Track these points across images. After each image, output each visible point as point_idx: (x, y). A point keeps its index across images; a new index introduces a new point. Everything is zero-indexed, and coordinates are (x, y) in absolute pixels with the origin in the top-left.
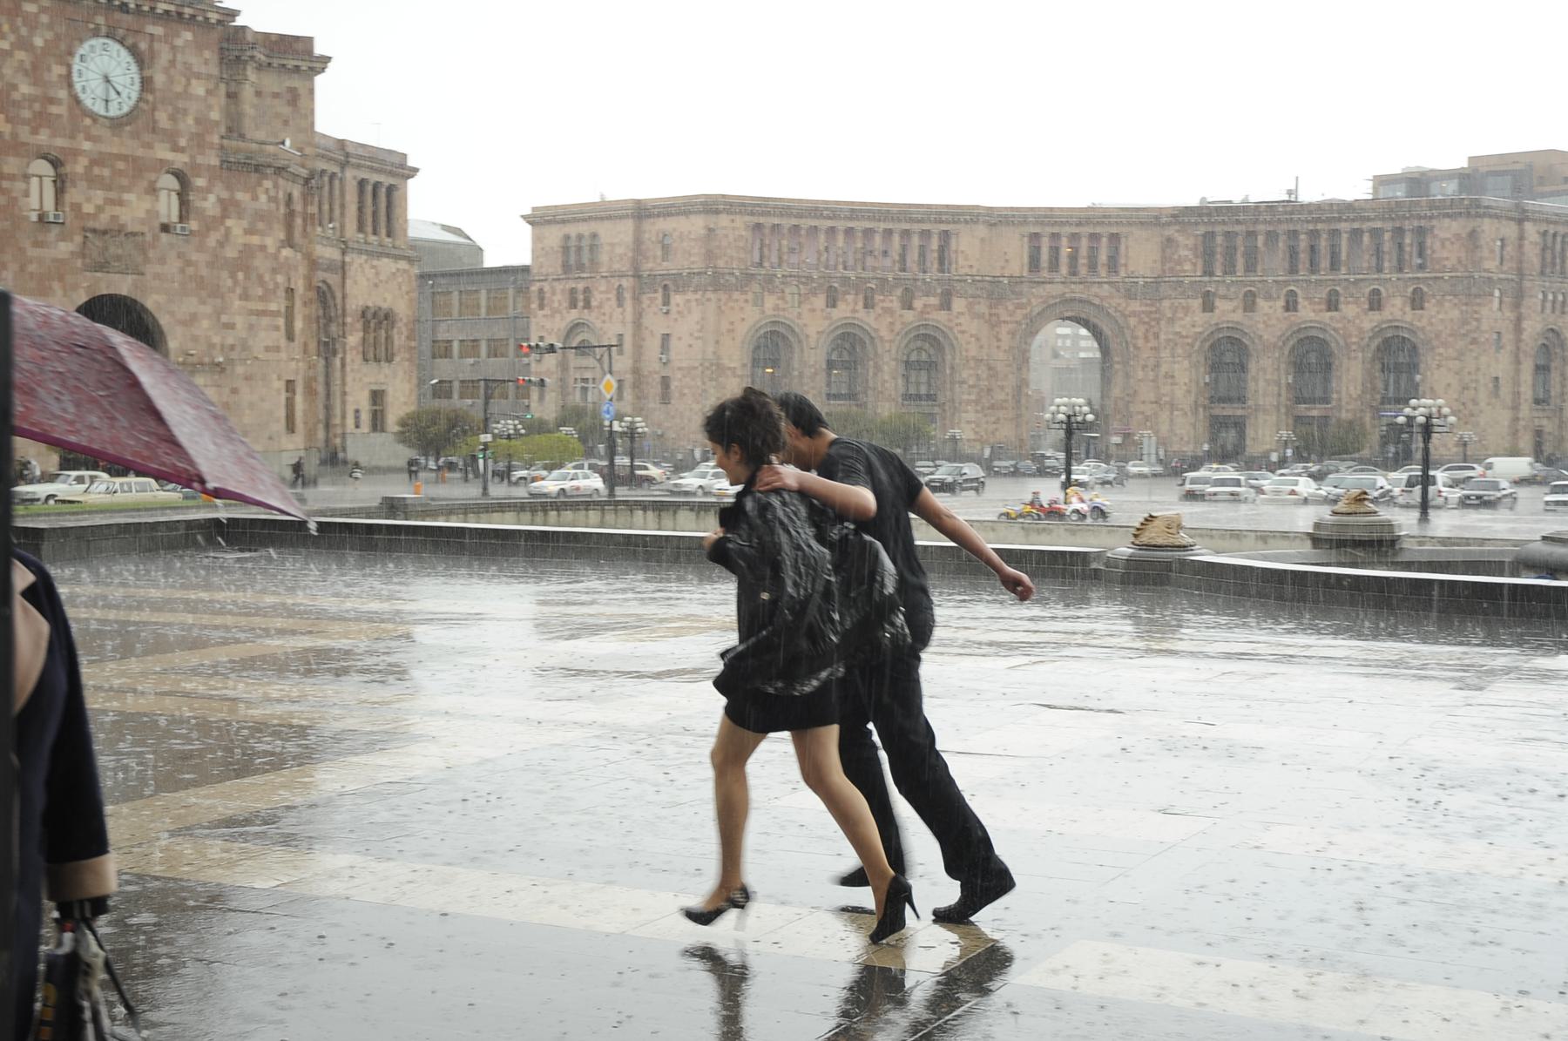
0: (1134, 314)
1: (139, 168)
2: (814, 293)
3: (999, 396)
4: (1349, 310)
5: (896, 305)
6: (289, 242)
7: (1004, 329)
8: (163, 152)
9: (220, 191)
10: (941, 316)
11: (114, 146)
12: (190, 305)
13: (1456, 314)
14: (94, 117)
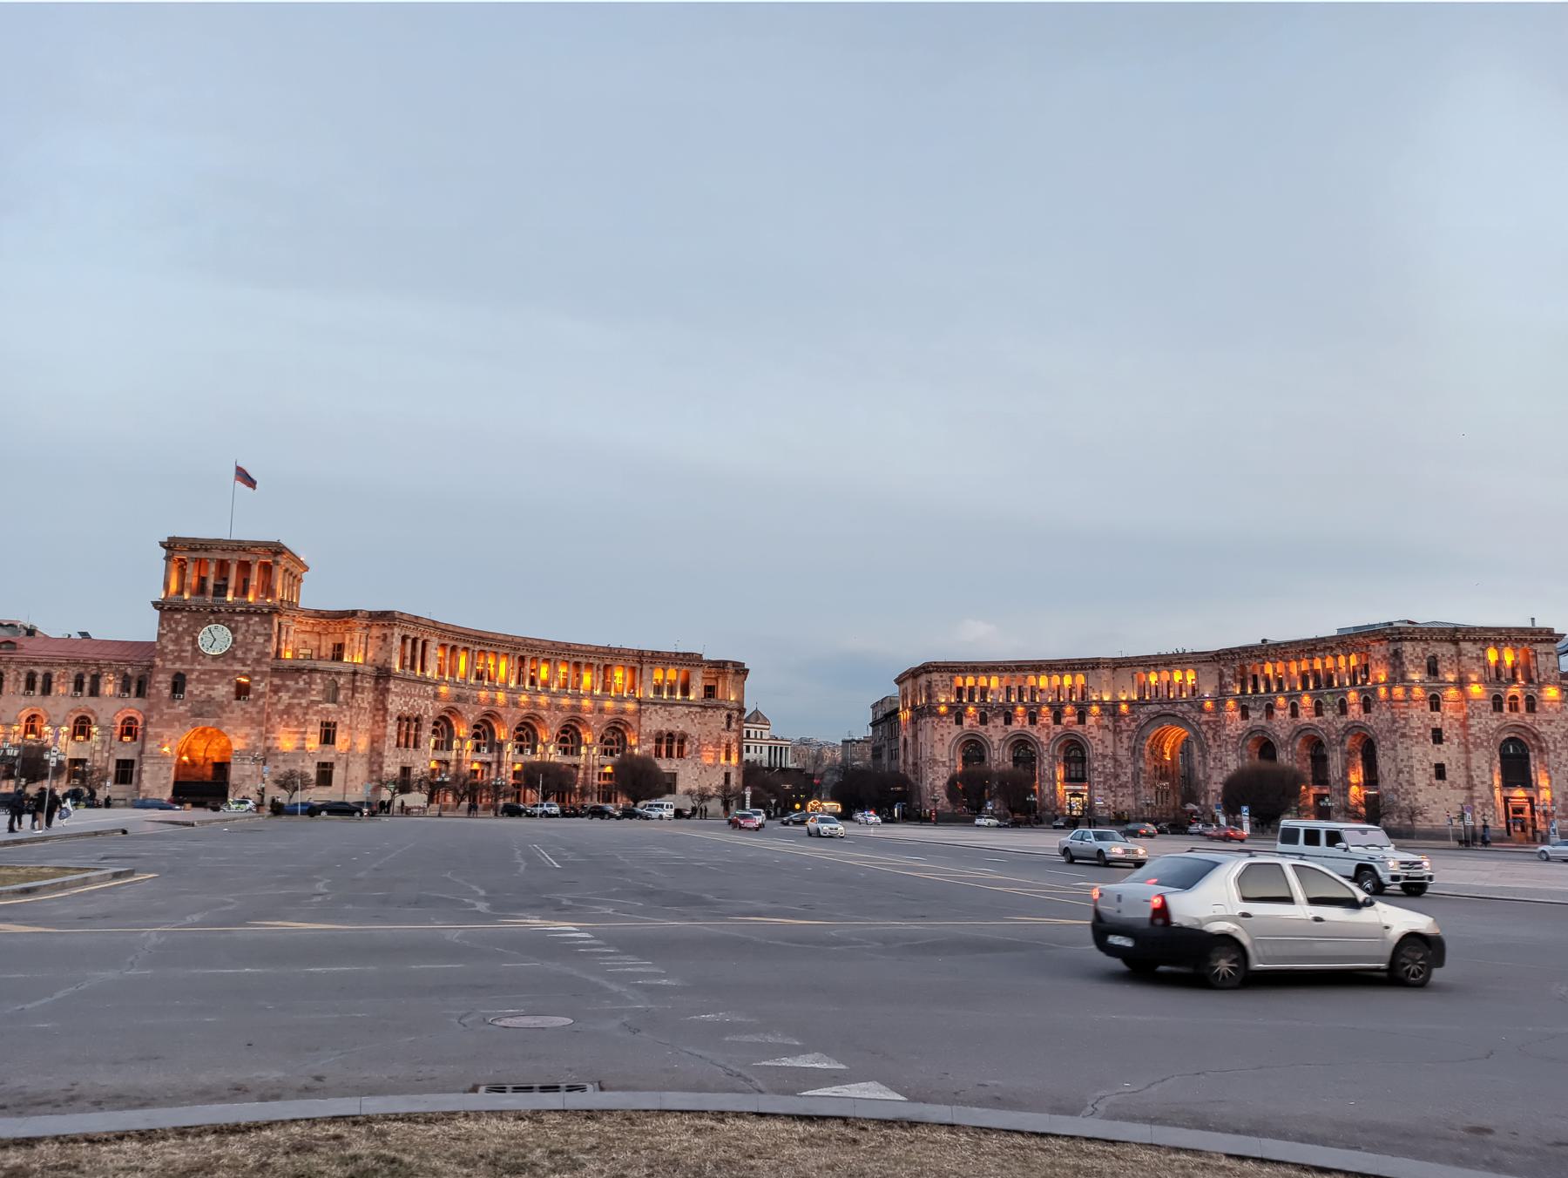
0: (1207, 723)
1: (223, 674)
2: (996, 716)
3: (1124, 779)
4: (1329, 715)
5: (1051, 722)
6: (334, 702)
7: (1125, 735)
8: (238, 667)
9: (277, 681)
10: (1079, 728)
11: (214, 666)
12: (246, 730)
13: (1388, 715)
14: (204, 655)
